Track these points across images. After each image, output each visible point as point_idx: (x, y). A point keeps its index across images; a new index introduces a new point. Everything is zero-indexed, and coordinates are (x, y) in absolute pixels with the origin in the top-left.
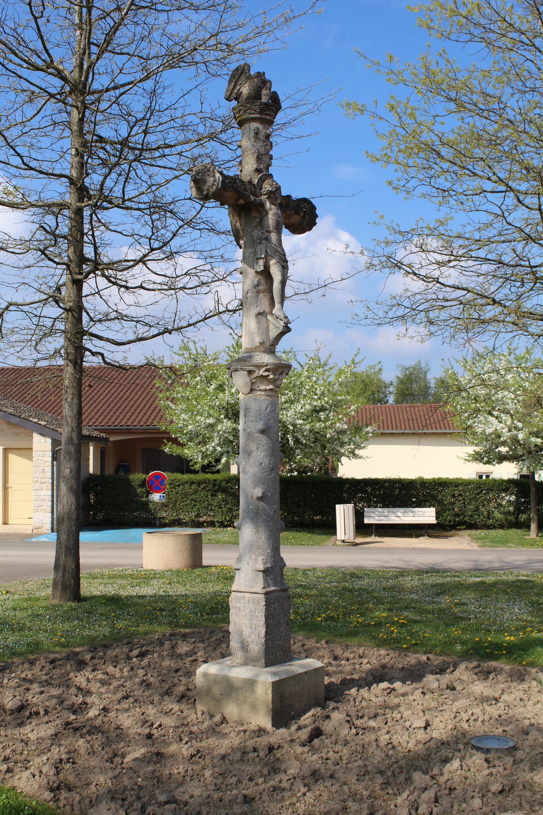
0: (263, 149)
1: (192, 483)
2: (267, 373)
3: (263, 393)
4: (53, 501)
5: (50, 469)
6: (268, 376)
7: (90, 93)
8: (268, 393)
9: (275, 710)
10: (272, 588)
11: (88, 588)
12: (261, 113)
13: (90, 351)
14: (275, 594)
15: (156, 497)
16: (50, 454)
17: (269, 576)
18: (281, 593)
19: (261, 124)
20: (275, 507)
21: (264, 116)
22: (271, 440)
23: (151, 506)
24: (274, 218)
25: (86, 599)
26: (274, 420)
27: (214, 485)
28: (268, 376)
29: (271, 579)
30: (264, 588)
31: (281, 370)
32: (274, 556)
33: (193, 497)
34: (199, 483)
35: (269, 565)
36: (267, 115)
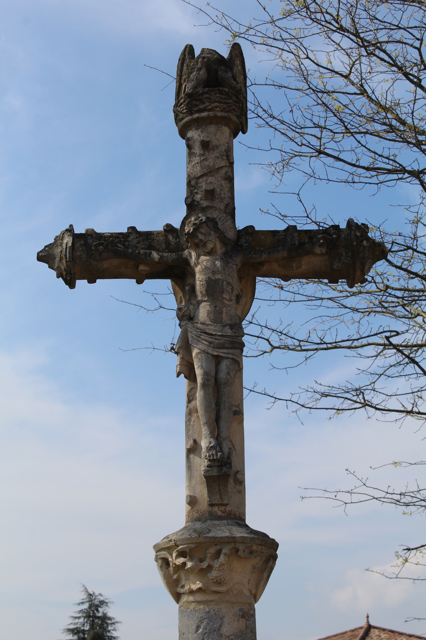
0: (199, 168)
2: (181, 560)
3: (191, 598)
6: (184, 564)
8: (199, 597)
12: (190, 112)
19: (197, 129)
24: (202, 277)
28: (184, 564)
31: (212, 550)
36: (200, 111)
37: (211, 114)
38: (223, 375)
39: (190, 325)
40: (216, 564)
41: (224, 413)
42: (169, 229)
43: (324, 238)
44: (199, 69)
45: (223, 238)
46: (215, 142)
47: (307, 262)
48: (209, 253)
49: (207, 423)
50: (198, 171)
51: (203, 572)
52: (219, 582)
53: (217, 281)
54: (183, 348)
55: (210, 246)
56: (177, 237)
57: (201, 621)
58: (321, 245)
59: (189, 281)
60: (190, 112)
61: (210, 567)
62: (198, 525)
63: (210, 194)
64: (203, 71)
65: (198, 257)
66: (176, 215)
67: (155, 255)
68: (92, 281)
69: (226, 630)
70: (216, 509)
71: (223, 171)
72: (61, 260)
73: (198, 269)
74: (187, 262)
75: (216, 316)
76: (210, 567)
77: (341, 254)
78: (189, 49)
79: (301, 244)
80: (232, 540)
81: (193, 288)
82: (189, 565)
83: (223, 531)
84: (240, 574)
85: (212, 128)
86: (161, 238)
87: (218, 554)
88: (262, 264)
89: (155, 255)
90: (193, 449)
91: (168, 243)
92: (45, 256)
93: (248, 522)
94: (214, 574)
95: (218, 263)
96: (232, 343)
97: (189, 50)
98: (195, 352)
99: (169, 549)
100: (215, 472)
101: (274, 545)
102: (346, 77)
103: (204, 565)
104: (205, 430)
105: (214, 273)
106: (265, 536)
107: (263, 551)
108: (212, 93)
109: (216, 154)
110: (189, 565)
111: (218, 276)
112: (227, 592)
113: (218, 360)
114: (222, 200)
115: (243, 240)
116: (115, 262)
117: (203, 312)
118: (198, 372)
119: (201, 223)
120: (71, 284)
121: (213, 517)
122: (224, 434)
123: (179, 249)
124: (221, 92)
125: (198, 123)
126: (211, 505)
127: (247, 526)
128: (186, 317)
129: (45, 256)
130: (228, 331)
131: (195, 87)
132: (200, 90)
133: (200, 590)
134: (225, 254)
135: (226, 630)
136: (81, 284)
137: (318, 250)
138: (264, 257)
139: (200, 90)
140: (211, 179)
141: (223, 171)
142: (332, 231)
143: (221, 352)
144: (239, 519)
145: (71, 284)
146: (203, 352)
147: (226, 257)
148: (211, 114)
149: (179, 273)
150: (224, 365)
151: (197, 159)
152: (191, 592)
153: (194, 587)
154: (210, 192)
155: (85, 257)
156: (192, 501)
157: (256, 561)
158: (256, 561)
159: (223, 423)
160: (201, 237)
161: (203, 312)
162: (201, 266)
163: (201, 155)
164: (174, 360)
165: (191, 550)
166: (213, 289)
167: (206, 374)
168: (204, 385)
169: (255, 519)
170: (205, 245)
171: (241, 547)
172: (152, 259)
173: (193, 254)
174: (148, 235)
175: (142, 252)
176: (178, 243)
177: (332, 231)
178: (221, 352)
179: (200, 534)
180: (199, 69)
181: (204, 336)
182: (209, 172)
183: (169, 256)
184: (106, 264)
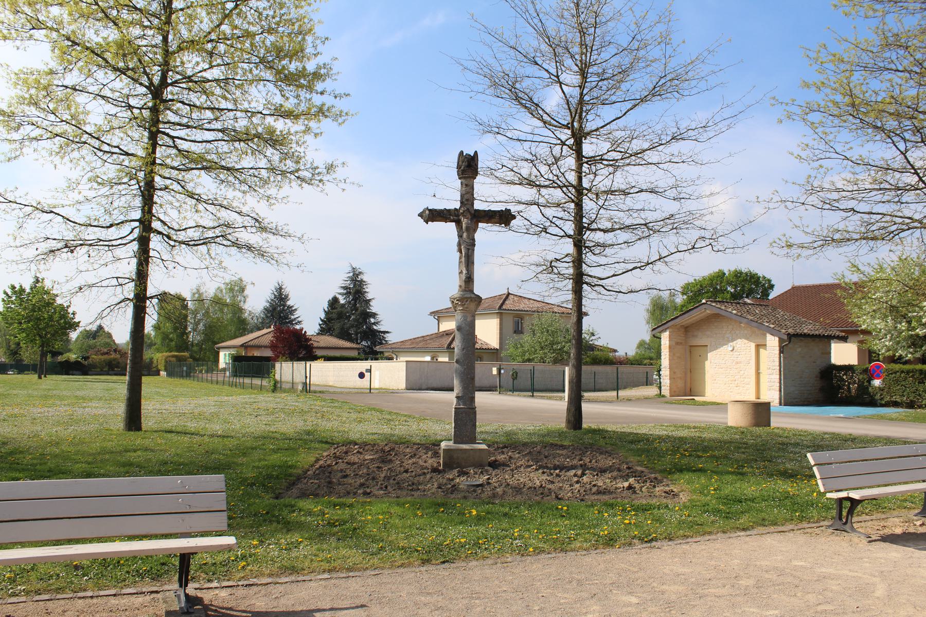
1: (902, 372)
4: (780, 383)
5: (777, 360)
13: (587, 283)
15: (877, 383)
16: (778, 348)
23: (870, 389)
27: (921, 374)
33: (903, 383)
34: (908, 372)
42: (456, 209)
45: (471, 214)
51: (463, 305)
54: (459, 245)
63: (467, 200)
66: (457, 205)
75: (468, 237)
77: (504, 218)
78: (462, 153)
83: (468, 295)
84: (472, 306)
90: (461, 273)
92: (421, 215)
93: (475, 292)
97: (462, 153)
108: (468, 167)
117: (465, 235)
123: (458, 216)
125: (464, 178)
128: (460, 236)
129: (421, 215)
144: (472, 291)
147: (471, 220)
149: (458, 223)
154: (467, 197)
155: (433, 216)
156: (460, 286)
161: (465, 235)
162: (465, 222)
164: (456, 248)
166: (468, 229)
169: (477, 291)
174: (449, 210)
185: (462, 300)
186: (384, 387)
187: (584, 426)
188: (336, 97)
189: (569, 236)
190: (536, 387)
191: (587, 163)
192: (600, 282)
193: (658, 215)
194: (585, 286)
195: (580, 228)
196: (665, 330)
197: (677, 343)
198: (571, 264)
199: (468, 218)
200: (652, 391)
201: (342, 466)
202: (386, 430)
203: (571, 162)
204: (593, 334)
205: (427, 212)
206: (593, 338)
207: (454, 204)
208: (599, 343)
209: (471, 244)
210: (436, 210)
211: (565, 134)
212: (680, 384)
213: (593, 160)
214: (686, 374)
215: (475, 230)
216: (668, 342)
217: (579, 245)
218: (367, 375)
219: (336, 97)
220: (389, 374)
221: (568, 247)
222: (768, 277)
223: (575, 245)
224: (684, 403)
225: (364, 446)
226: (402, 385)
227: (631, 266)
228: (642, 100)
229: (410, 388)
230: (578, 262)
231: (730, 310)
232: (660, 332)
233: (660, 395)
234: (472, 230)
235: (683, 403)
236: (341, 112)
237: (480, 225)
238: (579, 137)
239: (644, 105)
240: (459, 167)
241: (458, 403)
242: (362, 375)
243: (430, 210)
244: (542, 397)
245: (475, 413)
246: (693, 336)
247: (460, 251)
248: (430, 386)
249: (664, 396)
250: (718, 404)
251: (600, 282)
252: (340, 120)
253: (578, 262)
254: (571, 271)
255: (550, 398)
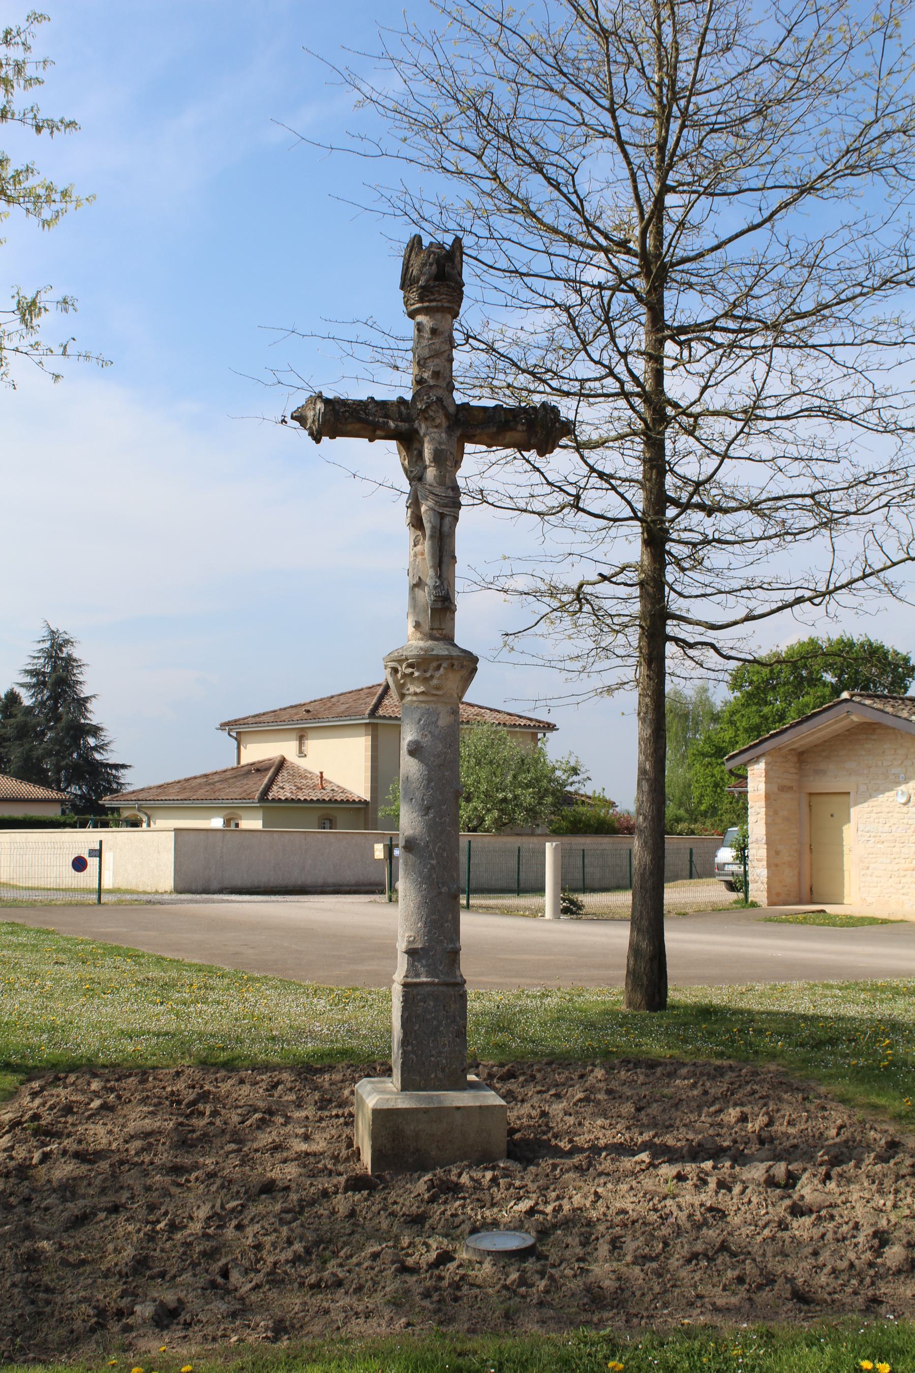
0: (427, 350)
2: (410, 670)
3: (415, 698)
6: (412, 673)
7: (617, 271)
8: (421, 698)
9: (380, 1151)
10: (425, 980)
11: (680, 992)
12: (421, 300)
13: (676, 640)
14: (429, 989)
17: (419, 961)
18: (441, 989)
20: (434, 862)
21: (426, 304)
22: (427, 765)
25: (673, 1007)
26: (433, 736)
28: (412, 673)
29: (423, 966)
30: (406, 976)
31: (435, 664)
32: (429, 932)
35: (419, 945)
36: (430, 301)
37: (439, 304)
38: (446, 529)
39: (419, 486)
40: (437, 674)
41: (445, 559)
42: (401, 401)
43: (526, 418)
44: (431, 265)
45: (447, 415)
46: (441, 329)
47: (509, 436)
48: (436, 427)
49: (433, 567)
50: (426, 353)
51: (425, 680)
52: (438, 688)
53: (442, 450)
54: (414, 503)
55: (438, 421)
56: (408, 408)
57: (422, 716)
58: (523, 424)
59: (416, 445)
60: (421, 300)
61: (432, 677)
62: (421, 644)
64: (434, 266)
65: (427, 428)
67: (392, 424)
68: (332, 437)
69: (441, 723)
70: (435, 632)
71: (446, 354)
72: (314, 421)
73: (426, 439)
74: (416, 432)
76: (432, 677)
77: (536, 430)
79: (507, 422)
80: (450, 657)
81: (420, 454)
82: (416, 674)
83: (441, 649)
84: (452, 682)
85: (439, 316)
86: (395, 409)
87: (438, 667)
88: (475, 436)
89: (392, 424)
90: (418, 584)
91: (400, 413)
93: (457, 641)
94: (435, 682)
95: (444, 435)
96: (454, 503)
98: (423, 508)
99: (400, 661)
100: (439, 605)
101: (475, 660)
102: (479, 157)
103: (428, 675)
104: (431, 572)
105: (440, 443)
106: (471, 654)
107: (467, 664)
108: (435, 280)
109: (441, 339)
110: (416, 674)
111: (443, 447)
112: (443, 696)
113: (442, 516)
114: (444, 378)
115: (460, 415)
116: (357, 426)
117: (431, 473)
118: (427, 526)
119: (432, 403)
120: (318, 441)
121: (432, 638)
122: (444, 576)
123: (409, 419)
124: (448, 286)
126: (432, 629)
127: (456, 646)
128: (415, 477)
130: (450, 493)
131: (427, 281)
132: (431, 283)
133: (423, 693)
134: (449, 427)
135: (441, 723)
136: (325, 439)
137: (520, 428)
138: (478, 431)
139: (431, 283)
140: (437, 361)
141: (446, 354)
142: (531, 411)
143: (445, 511)
144: (449, 639)
145: (318, 441)
146: (432, 509)
147: (450, 430)
148: (439, 304)
149: (408, 441)
150: (447, 520)
151: (425, 342)
152: (416, 694)
153: (418, 690)
157: (464, 673)
158: (464, 673)
159: (444, 567)
160: (431, 413)
161: (431, 473)
163: (429, 339)
165: (418, 663)
167: (433, 528)
168: (432, 537)
169: (461, 640)
170: (434, 420)
171: (456, 663)
172: (389, 427)
173: (423, 426)
174: (384, 404)
175: (381, 420)
176: (408, 414)
177: (531, 411)
178: (445, 511)
179: (426, 650)
180: (431, 265)
181: (431, 496)
182: (436, 355)
183: (404, 426)
184: (349, 428)
185: (424, 664)
186: (124, 886)
187: (674, 995)
188: (39, 129)
189: (636, 518)
190: (473, 884)
191: (672, 338)
192: (710, 636)
193: (838, 474)
194: (671, 648)
195: (659, 500)
196: (755, 760)
197: (783, 789)
198: (636, 591)
199: (431, 427)
200: (712, 892)
201: (64, 1170)
202: (160, 1017)
203: (634, 334)
204: (575, 771)
205: (320, 406)
206: (575, 778)
207: (395, 385)
208: (588, 789)
209: (449, 503)
210: (344, 403)
211: (628, 264)
212: (789, 876)
213: (685, 334)
214: (800, 854)
215: (457, 464)
216: (762, 786)
217: (656, 540)
218: (93, 862)
219: (39, 129)
220: (139, 858)
221: (629, 547)
222: (903, 651)
223: (647, 543)
224: (804, 920)
225: (117, 1076)
226: (167, 882)
227: (790, 596)
228: (805, 189)
229: (178, 890)
230: (653, 588)
231: (905, 714)
232: (746, 764)
233: (747, 903)
234: (449, 460)
235: (804, 922)
236: (49, 188)
237: (469, 447)
238: (657, 271)
239: (809, 200)
240: (407, 282)
241: (412, 970)
242: (79, 864)
243: (327, 402)
244: (488, 909)
245: (463, 997)
246: (818, 772)
247: (417, 523)
248: (227, 884)
249: (754, 905)
250: (884, 922)
251: (710, 636)
252: (47, 212)
253: (653, 588)
254: (636, 607)
255: (508, 912)
